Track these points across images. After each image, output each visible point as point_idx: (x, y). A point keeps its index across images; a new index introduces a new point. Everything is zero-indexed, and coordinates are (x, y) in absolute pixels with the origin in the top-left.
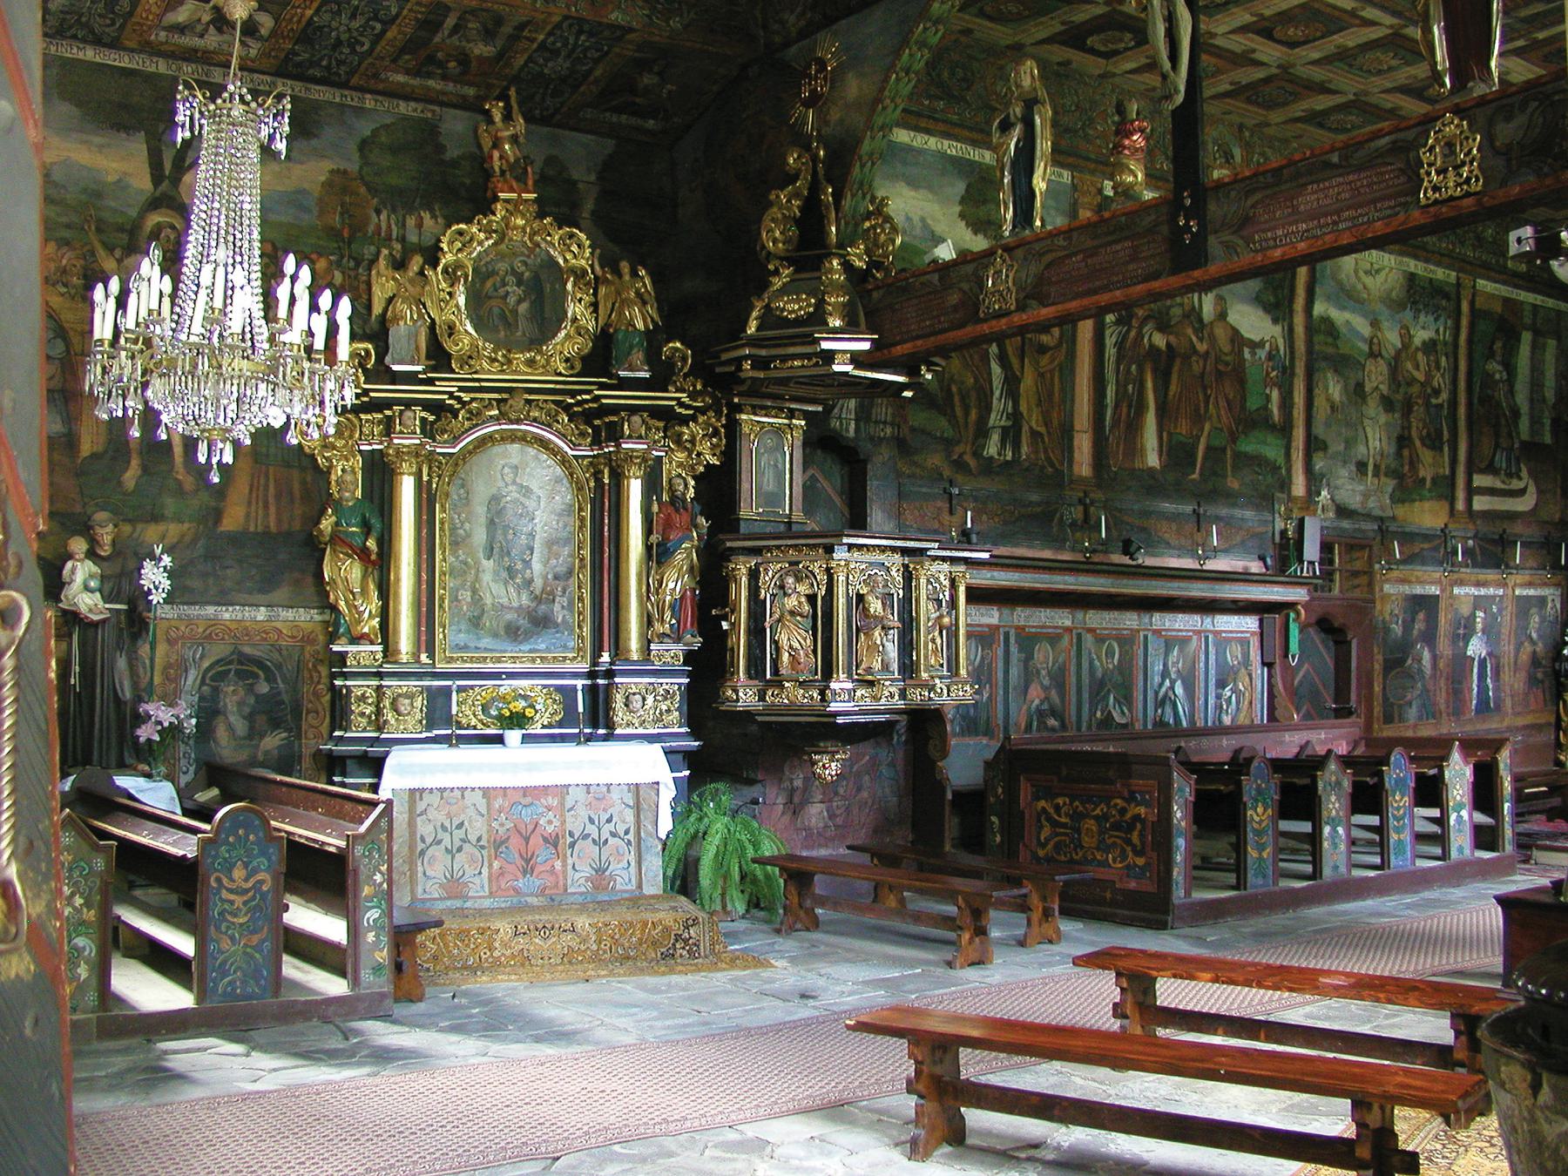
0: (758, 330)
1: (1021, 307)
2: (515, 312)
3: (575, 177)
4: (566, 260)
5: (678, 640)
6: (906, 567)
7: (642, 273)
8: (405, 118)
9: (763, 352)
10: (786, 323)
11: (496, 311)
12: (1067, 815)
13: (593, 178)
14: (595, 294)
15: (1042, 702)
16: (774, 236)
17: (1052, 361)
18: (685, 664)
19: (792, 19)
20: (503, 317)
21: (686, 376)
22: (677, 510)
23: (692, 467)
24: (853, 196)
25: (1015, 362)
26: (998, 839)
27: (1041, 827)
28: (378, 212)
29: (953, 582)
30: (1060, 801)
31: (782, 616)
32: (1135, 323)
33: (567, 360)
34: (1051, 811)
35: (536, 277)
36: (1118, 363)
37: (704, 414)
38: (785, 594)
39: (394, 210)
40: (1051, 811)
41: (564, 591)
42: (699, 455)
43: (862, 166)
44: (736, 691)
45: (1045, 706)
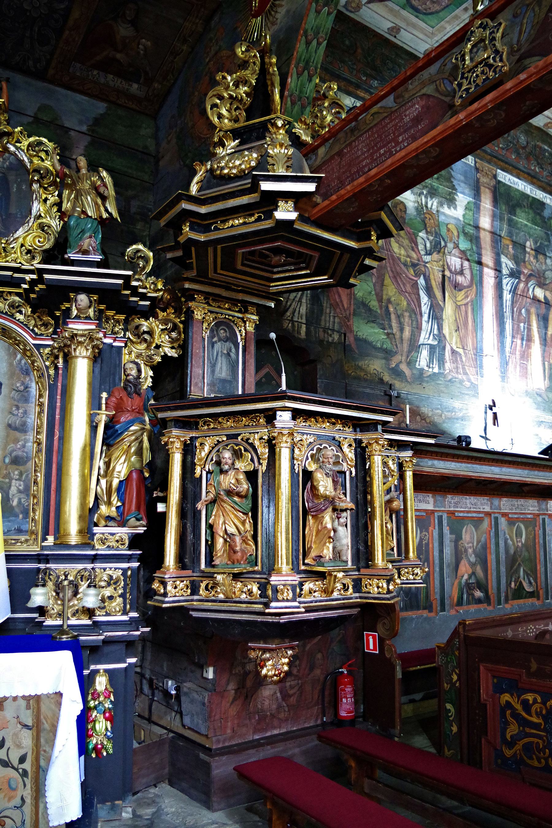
1: (519, 66)
3: (67, 124)
4: (31, 162)
5: (122, 524)
6: (358, 442)
7: (104, 174)
9: (203, 210)
10: (228, 179)
12: (538, 714)
13: (84, 128)
14: (60, 196)
15: (470, 577)
17: (467, 297)
18: (130, 548)
21: (149, 275)
22: (129, 394)
23: (150, 357)
24: (299, 74)
25: (438, 294)
26: (455, 729)
27: (507, 723)
29: (400, 466)
30: (530, 697)
31: (218, 495)
32: (523, 278)
33: (29, 252)
34: (518, 707)
36: (513, 303)
37: (164, 310)
38: (222, 472)
40: (518, 707)
41: (21, 474)
42: (158, 347)
43: (308, 43)
44: (164, 583)
45: (472, 581)
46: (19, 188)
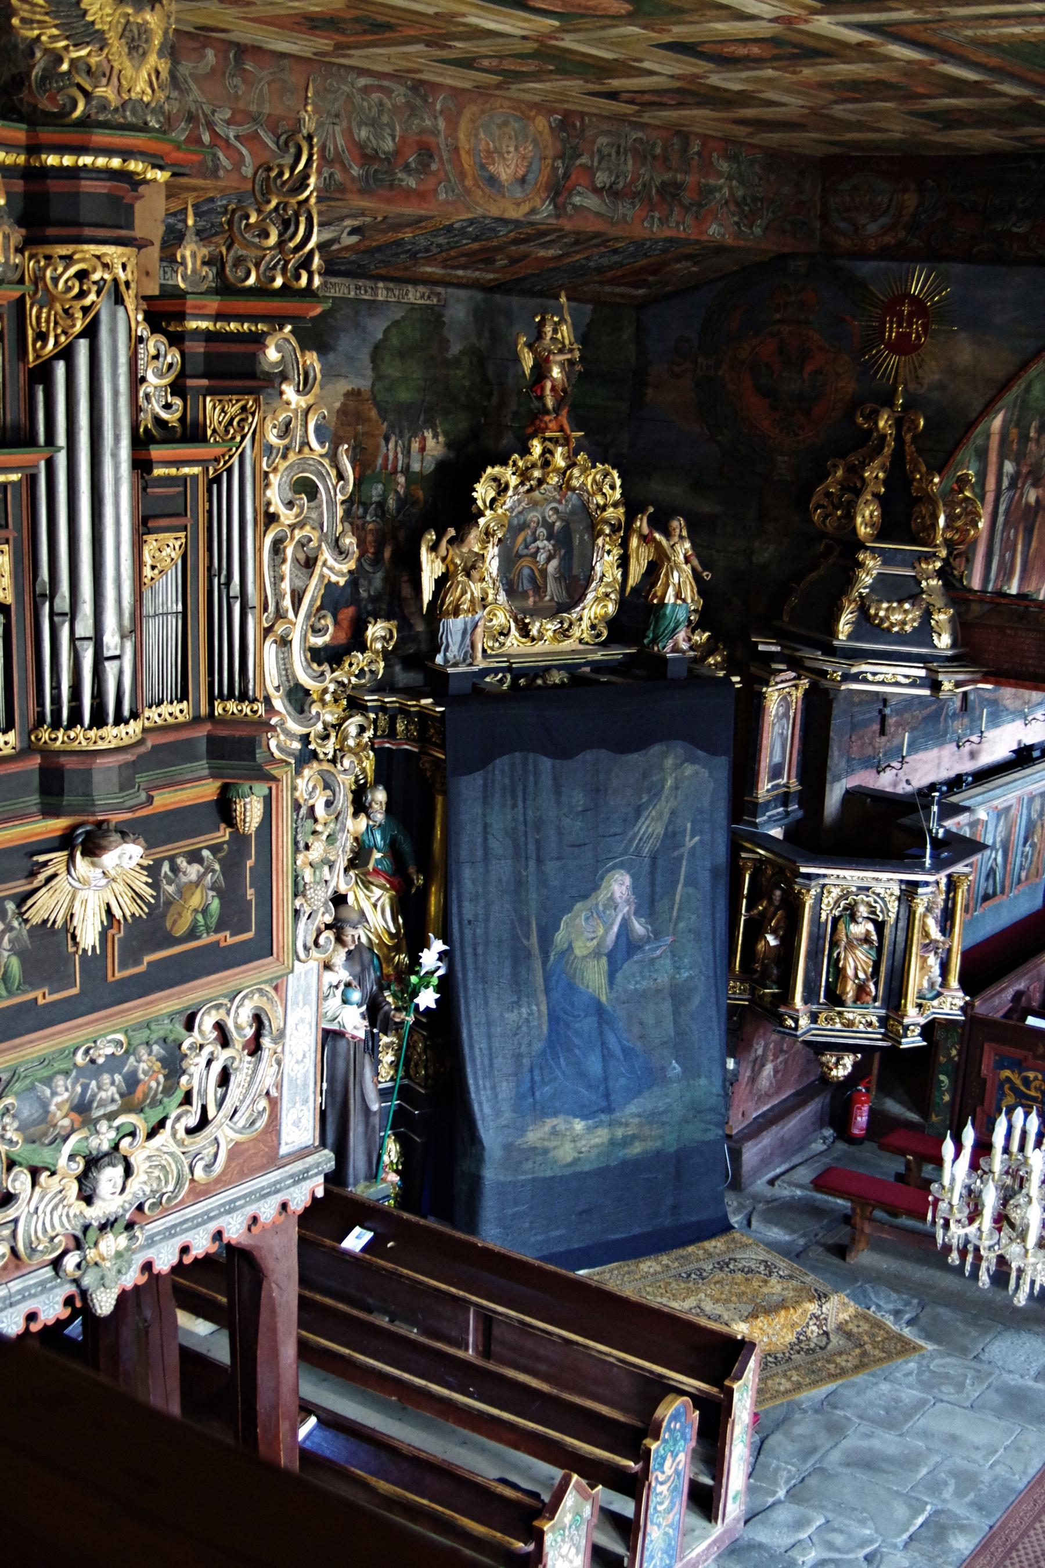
0: (850, 637)
2: (544, 572)
8: (413, 308)
11: (526, 572)
12: (1037, 1089)
16: (866, 518)
19: (873, 228)
20: (533, 579)
26: (947, 1098)
27: (1004, 1094)
28: (387, 440)
30: (1031, 1075)
34: (1018, 1082)
35: (567, 529)
39: (401, 436)
40: (1018, 1082)
44: (796, 1021)
46: (582, 539)
